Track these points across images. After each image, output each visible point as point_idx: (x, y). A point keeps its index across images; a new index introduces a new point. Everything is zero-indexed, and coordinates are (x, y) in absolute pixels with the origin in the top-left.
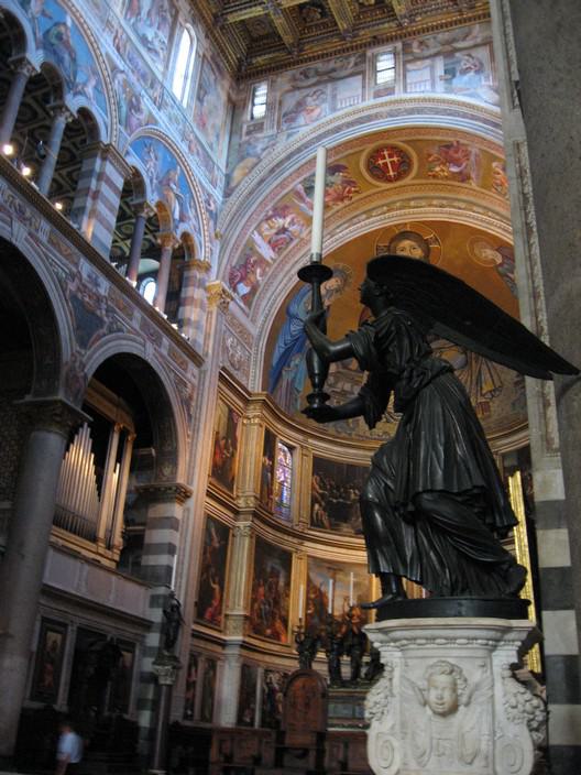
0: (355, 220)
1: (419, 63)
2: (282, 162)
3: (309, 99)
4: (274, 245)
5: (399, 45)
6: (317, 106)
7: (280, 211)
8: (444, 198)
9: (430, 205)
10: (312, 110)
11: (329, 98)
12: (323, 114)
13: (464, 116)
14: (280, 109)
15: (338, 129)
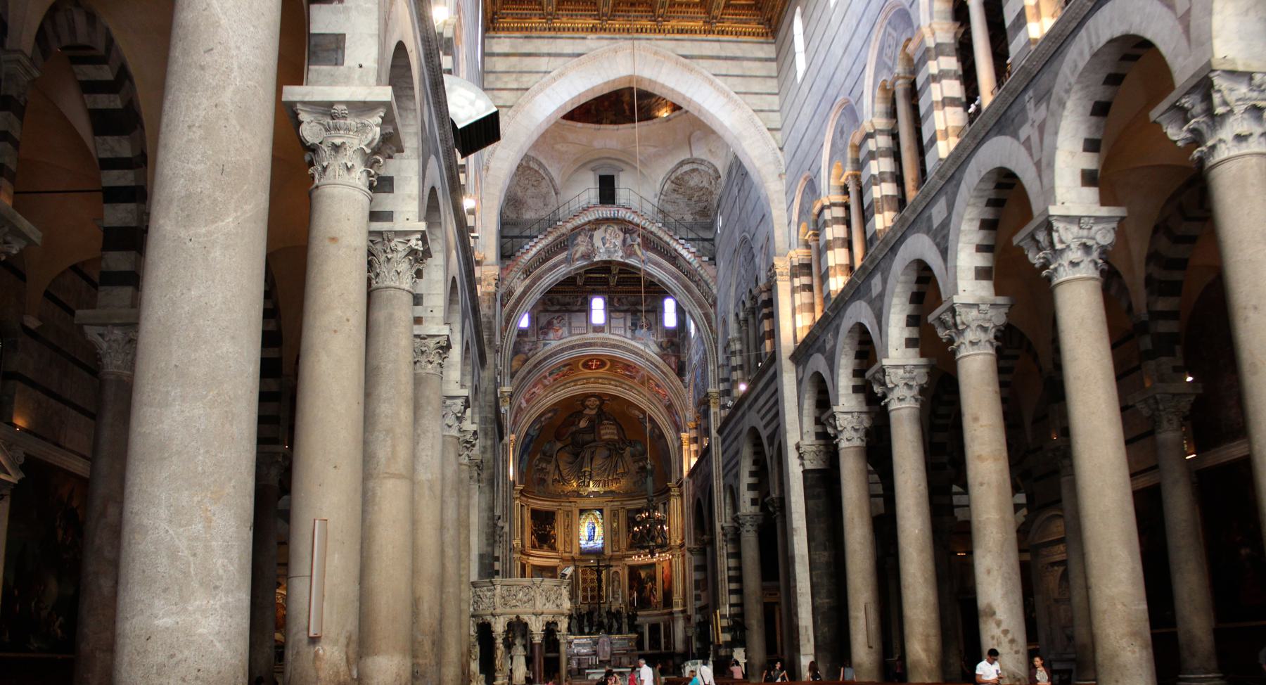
0: (568, 385)
1: (618, 314)
2: (540, 362)
3: (555, 321)
4: (528, 401)
5: (607, 297)
6: (561, 328)
7: (534, 386)
8: (618, 381)
9: (610, 384)
10: (557, 330)
11: (567, 324)
12: (564, 335)
13: (642, 356)
14: (537, 324)
15: (573, 347)
